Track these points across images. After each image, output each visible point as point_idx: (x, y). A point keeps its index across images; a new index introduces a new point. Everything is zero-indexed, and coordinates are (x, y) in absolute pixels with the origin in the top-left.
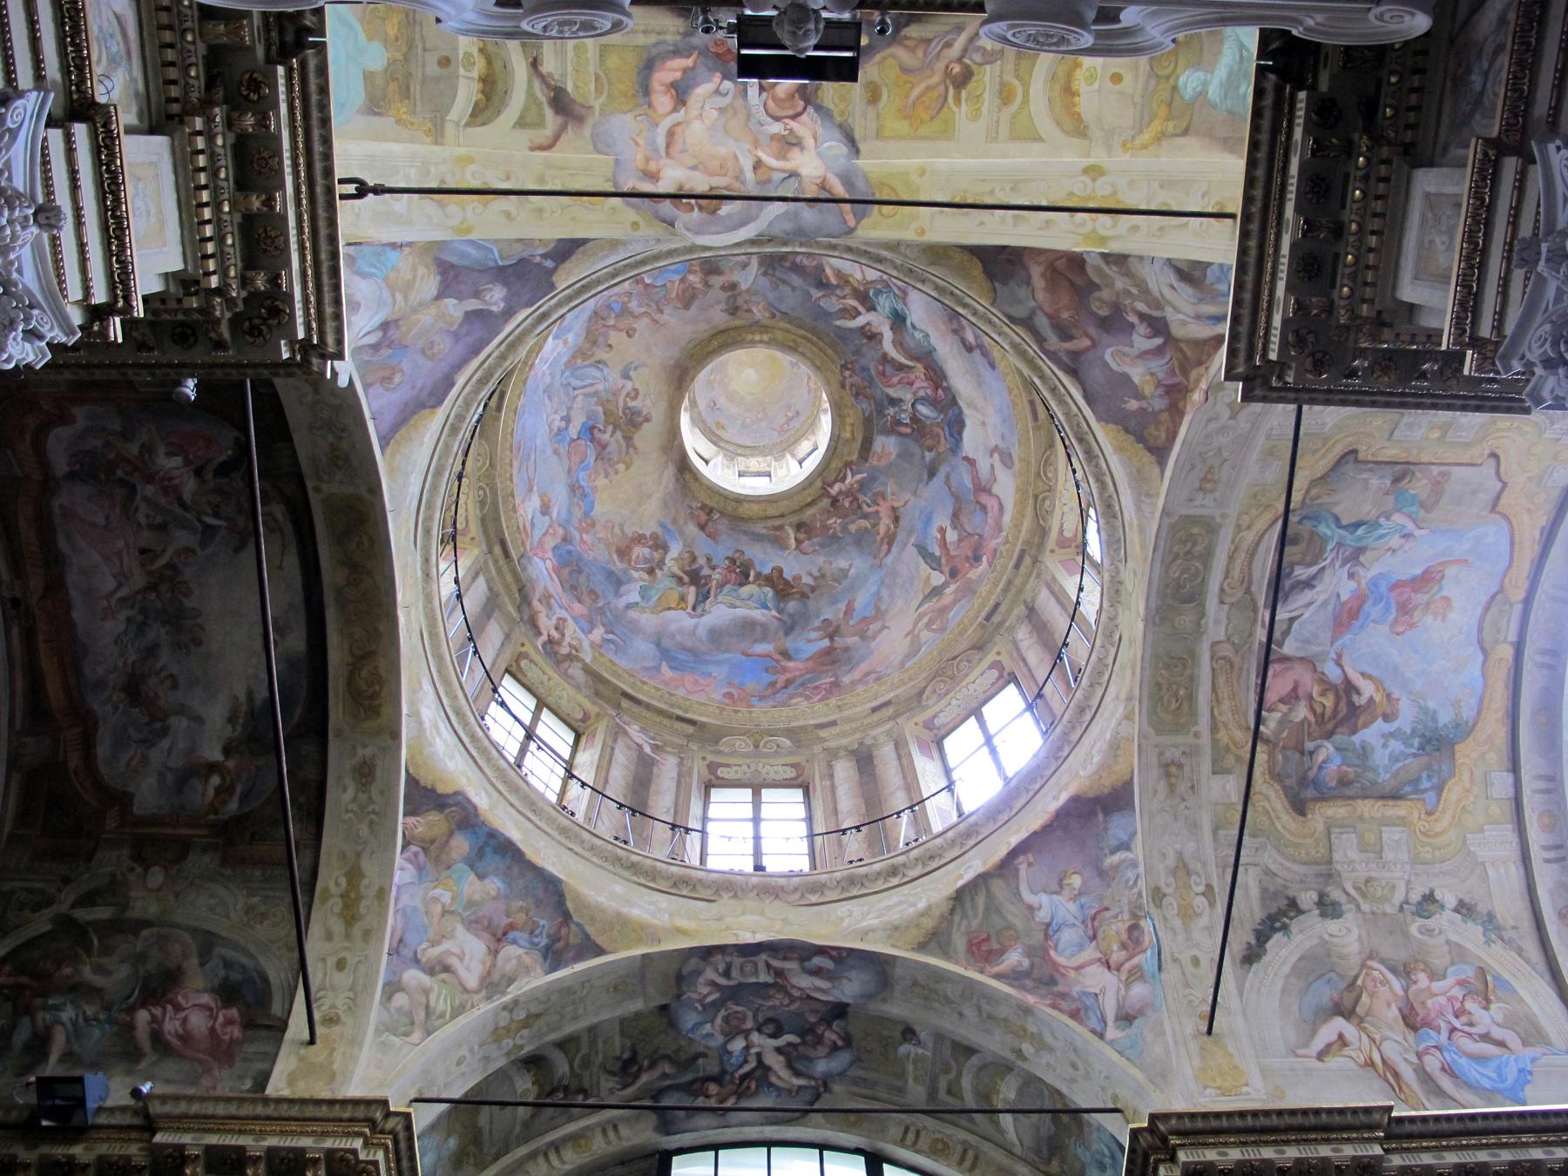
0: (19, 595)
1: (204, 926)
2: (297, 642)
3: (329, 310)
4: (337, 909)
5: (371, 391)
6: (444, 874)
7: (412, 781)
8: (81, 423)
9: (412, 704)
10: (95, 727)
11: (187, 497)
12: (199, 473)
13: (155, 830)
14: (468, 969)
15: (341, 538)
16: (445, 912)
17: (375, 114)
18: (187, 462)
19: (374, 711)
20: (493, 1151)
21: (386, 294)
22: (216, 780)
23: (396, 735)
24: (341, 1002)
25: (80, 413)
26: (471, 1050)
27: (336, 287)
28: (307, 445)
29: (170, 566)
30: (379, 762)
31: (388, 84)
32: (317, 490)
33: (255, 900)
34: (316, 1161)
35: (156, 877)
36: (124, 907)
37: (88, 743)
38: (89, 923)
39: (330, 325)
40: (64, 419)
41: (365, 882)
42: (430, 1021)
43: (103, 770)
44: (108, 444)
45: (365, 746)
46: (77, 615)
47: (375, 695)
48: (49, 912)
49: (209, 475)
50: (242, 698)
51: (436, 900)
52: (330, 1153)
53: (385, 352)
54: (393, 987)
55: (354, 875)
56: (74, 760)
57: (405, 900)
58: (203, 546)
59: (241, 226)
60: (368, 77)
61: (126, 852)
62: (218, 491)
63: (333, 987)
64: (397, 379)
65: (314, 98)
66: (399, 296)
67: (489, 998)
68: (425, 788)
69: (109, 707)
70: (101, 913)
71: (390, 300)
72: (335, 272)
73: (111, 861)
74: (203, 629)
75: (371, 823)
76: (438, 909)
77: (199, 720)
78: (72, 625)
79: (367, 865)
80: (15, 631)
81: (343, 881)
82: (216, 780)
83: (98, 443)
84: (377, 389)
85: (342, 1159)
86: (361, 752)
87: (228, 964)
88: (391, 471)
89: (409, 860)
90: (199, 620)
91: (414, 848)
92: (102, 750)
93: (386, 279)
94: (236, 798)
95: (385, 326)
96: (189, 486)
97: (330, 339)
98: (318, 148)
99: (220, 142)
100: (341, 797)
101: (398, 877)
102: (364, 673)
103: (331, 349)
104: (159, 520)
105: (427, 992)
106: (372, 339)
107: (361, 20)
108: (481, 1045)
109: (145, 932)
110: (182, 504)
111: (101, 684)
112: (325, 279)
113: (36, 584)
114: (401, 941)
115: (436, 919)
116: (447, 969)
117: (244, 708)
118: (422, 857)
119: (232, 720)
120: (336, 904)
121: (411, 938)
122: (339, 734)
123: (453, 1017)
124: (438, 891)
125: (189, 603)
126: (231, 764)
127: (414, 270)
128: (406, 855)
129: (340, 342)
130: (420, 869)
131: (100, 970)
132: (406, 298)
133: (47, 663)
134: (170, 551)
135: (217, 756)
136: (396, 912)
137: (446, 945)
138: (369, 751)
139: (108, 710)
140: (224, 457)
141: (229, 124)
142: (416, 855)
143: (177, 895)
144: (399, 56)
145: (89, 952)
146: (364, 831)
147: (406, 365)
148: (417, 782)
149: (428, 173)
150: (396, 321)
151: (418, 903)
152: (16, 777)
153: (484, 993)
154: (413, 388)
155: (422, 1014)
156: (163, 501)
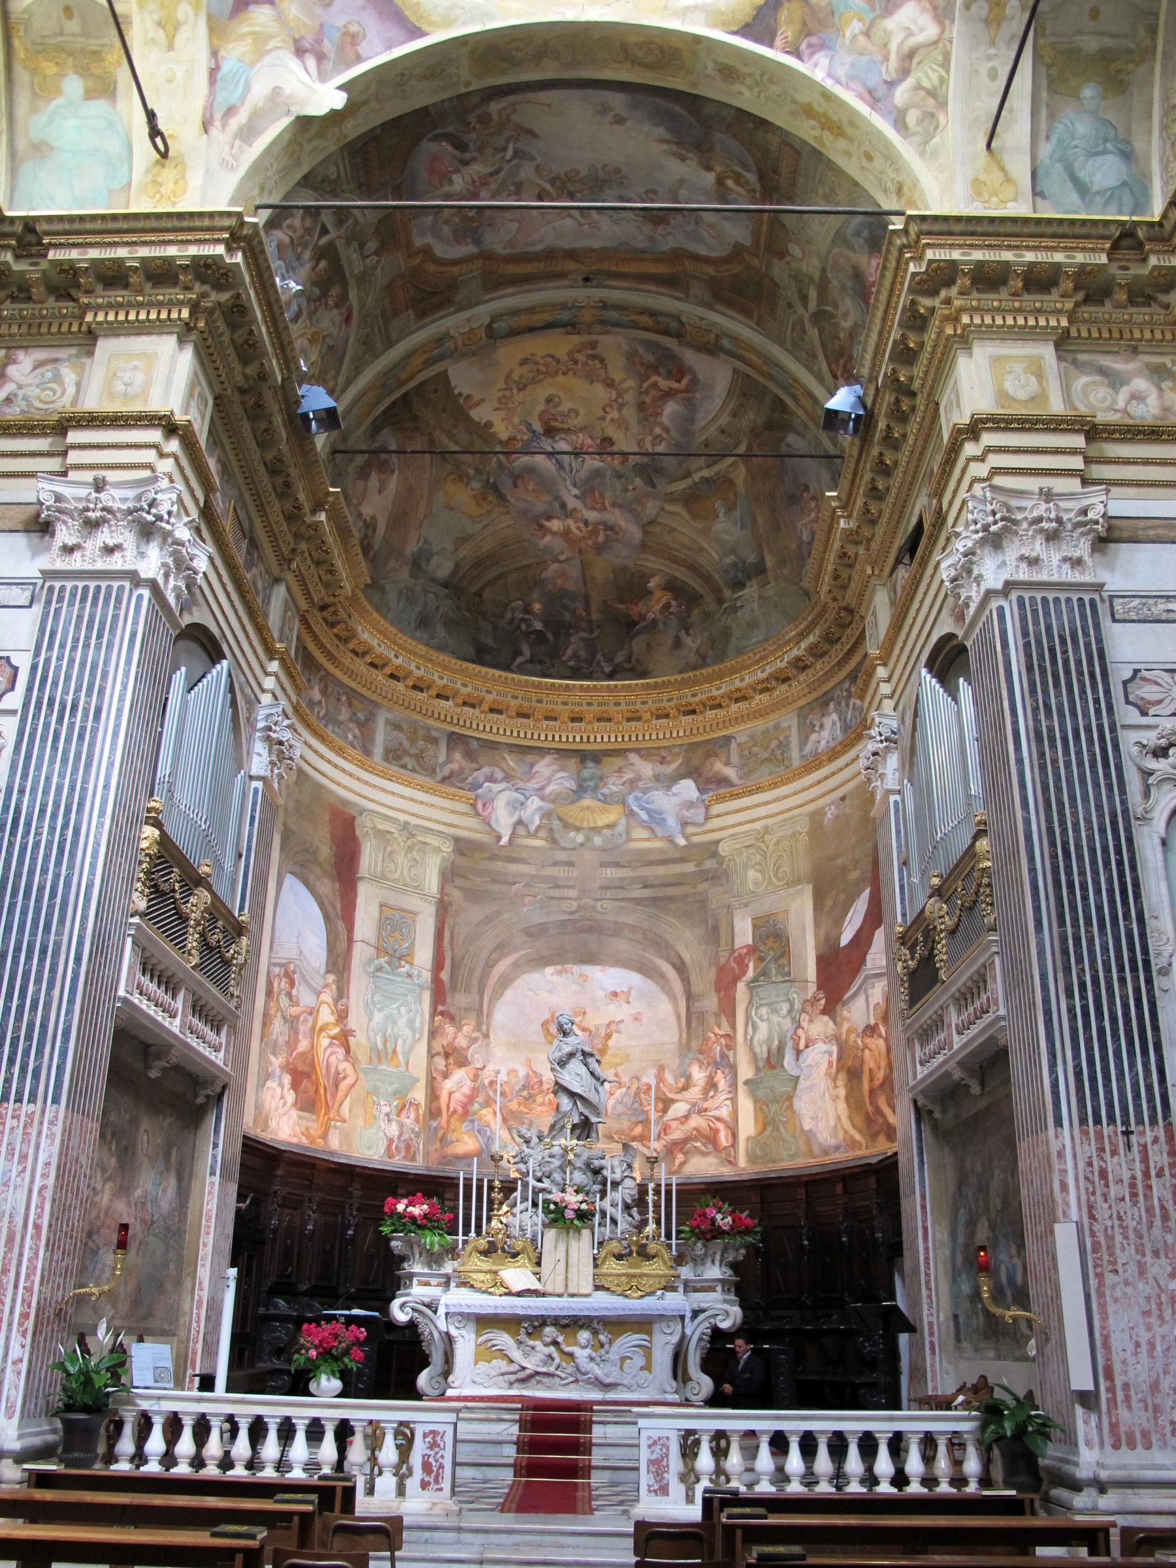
0: (580, 277)
1: (832, 235)
2: (618, 100)
3: (207, 222)
4: (831, 137)
5: (363, 55)
6: (836, 20)
7: (745, 31)
8: (430, 240)
9: (674, 14)
10: (686, 251)
11: (488, 170)
12: (466, 163)
13: (763, 237)
14: (922, 30)
15: (514, 63)
16: (867, 34)
17: (115, 89)
18: (457, 171)
19: (676, 52)
20: (1142, 33)
21: (268, 60)
22: (730, 183)
23: (697, 39)
24: (892, 174)
25: (418, 242)
26: (989, 58)
27: (192, 215)
28: (422, 97)
29: (552, 182)
30: (719, 59)
31: (92, 75)
32: (468, 84)
33: (820, 191)
34: (913, 303)
35: (795, 249)
36: (811, 279)
37: (697, 258)
38: (818, 305)
39: (218, 222)
40: (427, 251)
41: (815, 105)
42: (938, 96)
43: (716, 254)
44: (446, 222)
45: (706, 67)
46: (596, 244)
47: (661, 49)
48: (808, 326)
49: (467, 156)
50: (664, 147)
51: (855, 36)
52: (911, 290)
53: (328, 46)
54: (900, 124)
55: (808, 112)
56: (710, 270)
57: (841, 72)
58: (533, 159)
59: (154, 286)
60: (89, 95)
61: (776, 261)
62: (481, 148)
63: (882, 173)
64: (354, 28)
65: (67, 226)
66: (271, 45)
67: (953, 21)
68: (755, 18)
69: (670, 238)
70: (813, 294)
71: (274, 54)
72: (180, 216)
73: (779, 271)
74: (605, 166)
75: (770, 81)
76: (862, 39)
77: (682, 181)
78: (603, 249)
79: (804, 97)
80: (608, 283)
81: (813, 123)
82: (730, 183)
83: (446, 228)
84: (363, 49)
85: (919, 283)
86: (710, 71)
87: (857, 234)
88: (447, 23)
89: (812, 55)
90: (599, 166)
91: (803, 47)
92: (703, 251)
93: (252, 65)
94: (746, 174)
95: (300, 52)
96: (478, 169)
97: (227, 222)
98: (98, 225)
99: (100, 301)
100: (746, 99)
101: (819, 75)
102: (641, 54)
103: (232, 222)
104: (512, 188)
105: (918, 87)
106: (311, 62)
107: (48, 101)
108: (993, 43)
109: (829, 275)
110: (497, 172)
111: (651, 239)
112: (185, 224)
113: (570, 265)
114: (870, 92)
115: (869, 46)
116: (911, 55)
117: (674, 148)
118: (814, 40)
119: (683, 159)
120: (827, 136)
121: (873, 80)
122: (694, 85)
123: (948, 71)
124: (848, 34)
125: (584, 172)
126: (719, 169)
127: (245, 35)
128: (805, 58)
129: (229, 214)
130: (822, 46)
131: (845, 315)
132: (271, 37)
133: (634, 268)
134: (538, 181)
135: (710, 178)
136: (847, 87)
137: (893, 47)
138: (710, 65)
139: (670, 239)
140: (450, 147)
141: (89, 292)
142: (810, 46)
143: (809, 242)
144: (70, 61)
145: (832, 316)
146: (775, 89)
147: (340, 21)
148: (747, 25)
149: (153, 40)
150: (295, 41)
151: (849, 59)
152: (718, 307)
153: (947, 22)
154: (364, 8)
155: (931, 101)
156: (494, 186)
